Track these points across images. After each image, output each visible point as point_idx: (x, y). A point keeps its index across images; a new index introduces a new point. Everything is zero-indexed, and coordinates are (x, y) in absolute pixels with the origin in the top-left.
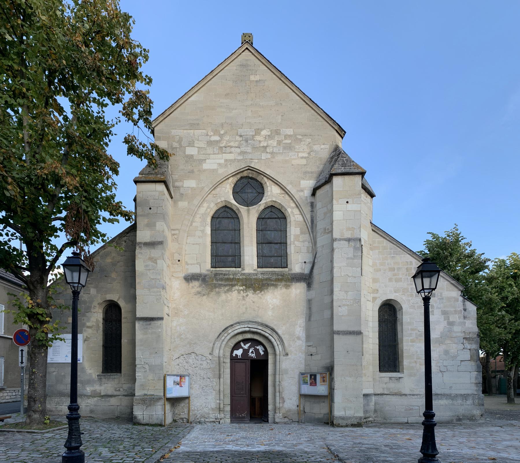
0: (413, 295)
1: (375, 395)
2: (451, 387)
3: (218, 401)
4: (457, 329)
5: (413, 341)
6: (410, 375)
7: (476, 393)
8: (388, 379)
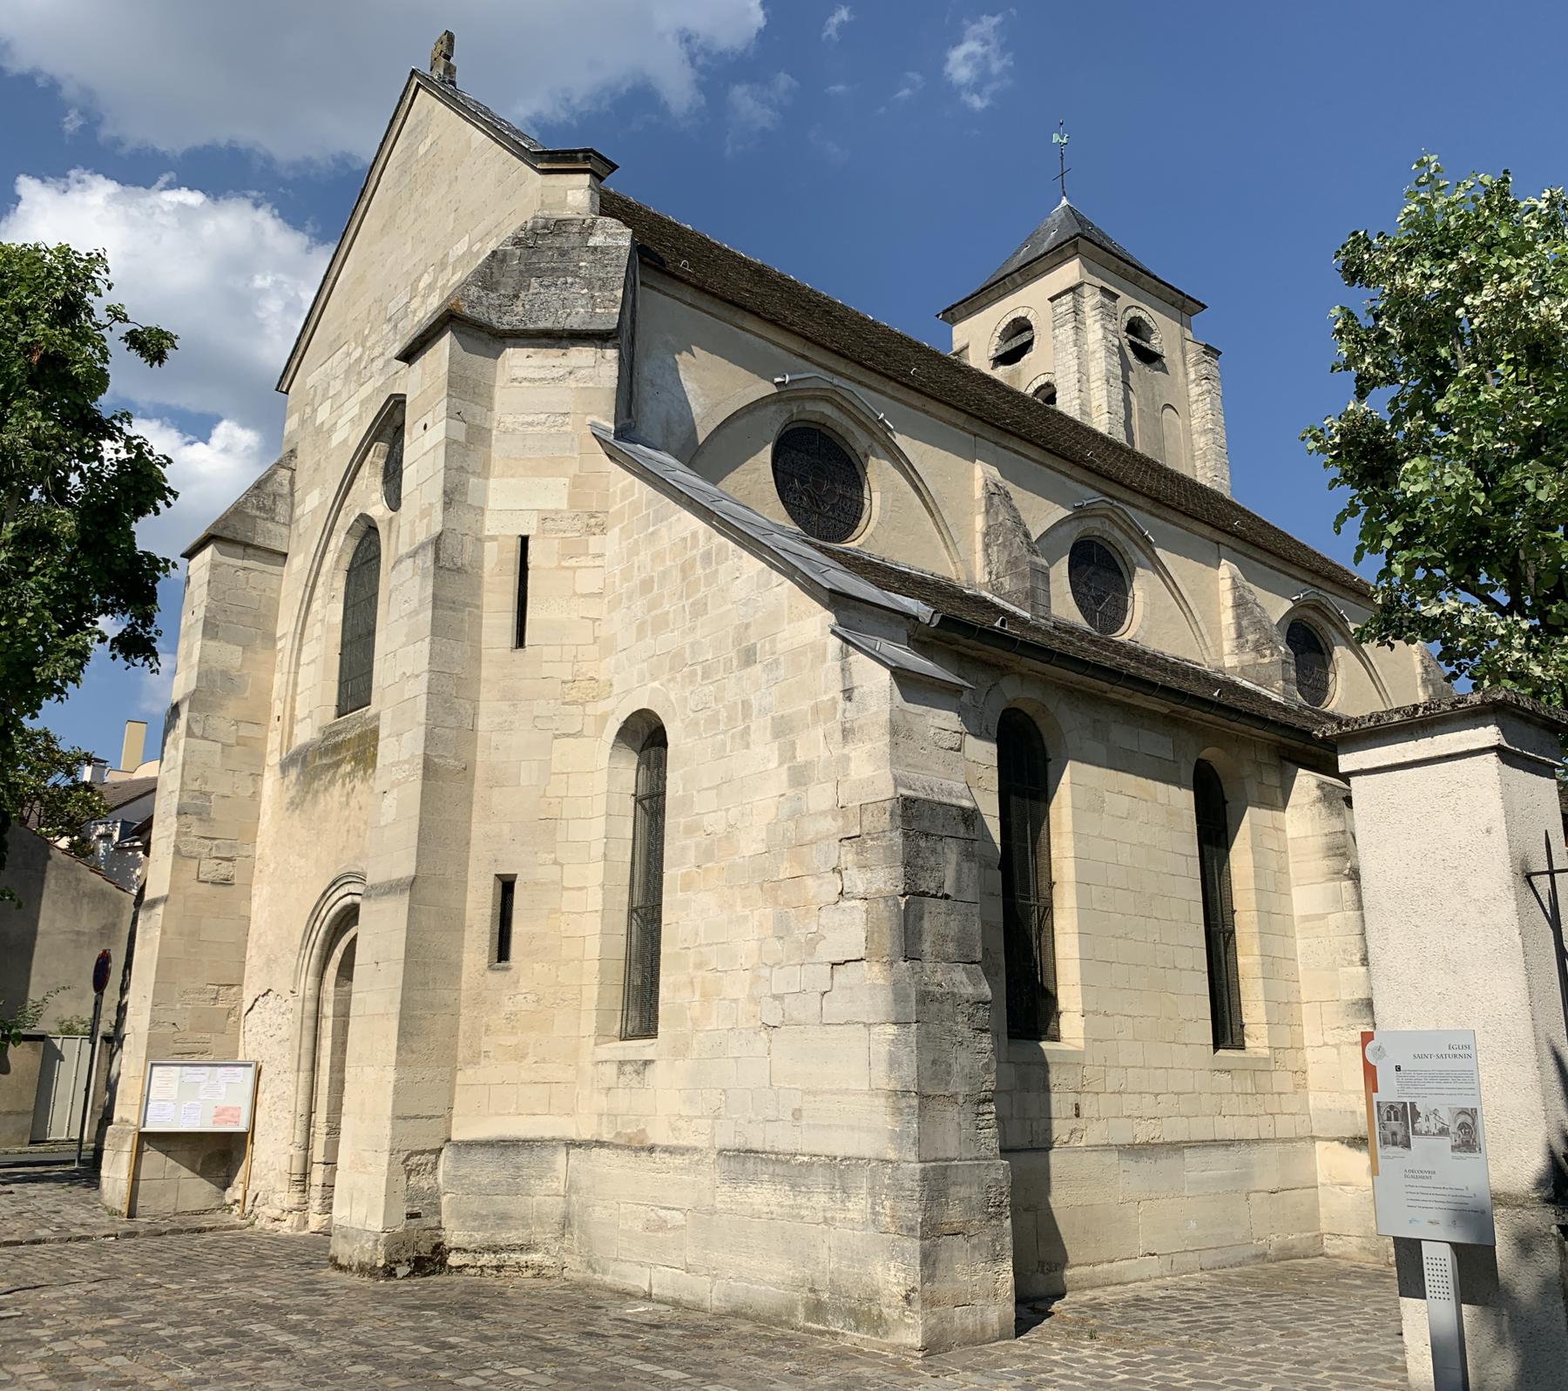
0: (694, 673)
1: (572, 1144)
2: (797, 1114)
3: (292, 1151)
4: (820, 797)
5: (687, 885)
6: (680, 1050)
7: (892, 1155)
8: (615, 1067)
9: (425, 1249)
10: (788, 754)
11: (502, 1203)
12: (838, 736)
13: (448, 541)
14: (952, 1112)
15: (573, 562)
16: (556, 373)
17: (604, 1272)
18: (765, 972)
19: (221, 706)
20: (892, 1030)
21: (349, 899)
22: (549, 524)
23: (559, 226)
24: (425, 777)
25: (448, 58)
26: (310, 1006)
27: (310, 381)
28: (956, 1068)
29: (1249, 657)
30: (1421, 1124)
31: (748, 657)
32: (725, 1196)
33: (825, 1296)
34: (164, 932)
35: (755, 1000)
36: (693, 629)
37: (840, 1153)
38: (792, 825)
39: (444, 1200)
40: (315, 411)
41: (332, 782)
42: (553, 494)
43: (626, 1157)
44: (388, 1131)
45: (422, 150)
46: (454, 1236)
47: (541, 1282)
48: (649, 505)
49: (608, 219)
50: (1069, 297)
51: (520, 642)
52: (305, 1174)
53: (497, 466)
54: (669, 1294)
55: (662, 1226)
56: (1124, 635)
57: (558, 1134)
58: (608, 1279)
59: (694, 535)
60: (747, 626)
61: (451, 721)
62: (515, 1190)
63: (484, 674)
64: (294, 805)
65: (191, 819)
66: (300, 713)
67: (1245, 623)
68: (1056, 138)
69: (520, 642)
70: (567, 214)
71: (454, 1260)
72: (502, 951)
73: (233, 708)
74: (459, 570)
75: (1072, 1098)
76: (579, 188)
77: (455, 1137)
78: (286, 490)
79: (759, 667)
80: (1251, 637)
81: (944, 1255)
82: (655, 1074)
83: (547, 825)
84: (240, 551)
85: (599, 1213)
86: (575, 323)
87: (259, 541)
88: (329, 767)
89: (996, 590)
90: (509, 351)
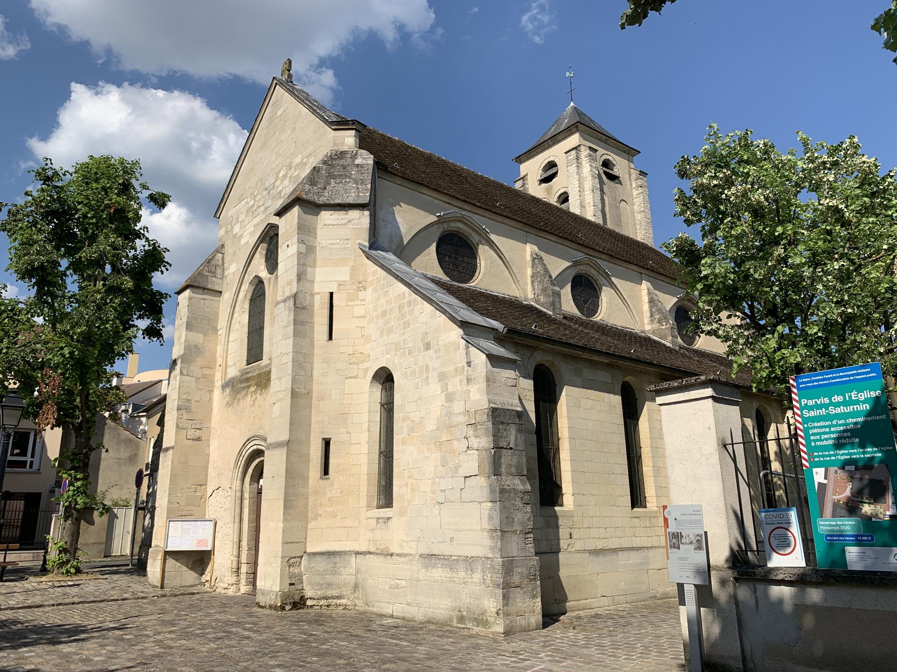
2: (452, 539)
4: (458, 407)
6: (402, 513)
7: (490, 555)
9: (297, 598)
10: (445, 388)
11: (329, 578)
12: (465, 381)
13: (300, 295)
14: (515, 538)
15: (352, 303)
16: (343, 222)
17: (373, 606)
18: (437, 480)
19: (194, 361)
20: (490, 504)
21: (255, 447)
22: (342, 287)
23: (342, 154)
24: (292, 397)
25: (289, 71)
26: (239, 494)
27: (230, 213)
28: (516, 519)
29: (656, 326)
30: (684, 540)
31: (428, 346)
32: (423, 574)
33: (465, 613)
34: (172, 462)
35: (434, 492)
36: (404, 333)
37: (470, 555)
38: (447, 418)
39: (304, 577)
40: (232, 227)
41: (246, 395)
42: (343, 274)
43: (381, 558)
44: (281, 549)
45: (279, 113)
46: (308, 593)
47: (347, 612)
48: (384, 279)
49: (363, 151)
50: (574, 152)
51: (331, 337)
52: (238, 568)
53: (319, 263)
54: (400, 615)
55: (397, 586)
56: (598, 318)
57: (352, 549)
58: (375, 610)
59: (404, 293)
60: (427, 333)
61: (302, 373)
62: (334, 572)
63: (316, 352)
64: (229, 405)
65: (183, 411)
66: (230, 363)
67: (654, 310)
68: (568, 74)
69: (331, 338)
70: (345, 148)
71: (309, 603)
72: (326, 471)
73: (200, 361)
74: (304, 308)
75: (568, 530)
76: (350, 136)
77: (309, 550)
78: (220, 263)
79: (432, 351)
80: (657, 317)
81: (512, 596)
82: (393, 523)
83: (343, 416)
84: (201, 291)
85: (370, 582)
86: (350, 200)
87: (209, 286)
88: (244, 388)
89: (537, 302)
90: (323, 212)
